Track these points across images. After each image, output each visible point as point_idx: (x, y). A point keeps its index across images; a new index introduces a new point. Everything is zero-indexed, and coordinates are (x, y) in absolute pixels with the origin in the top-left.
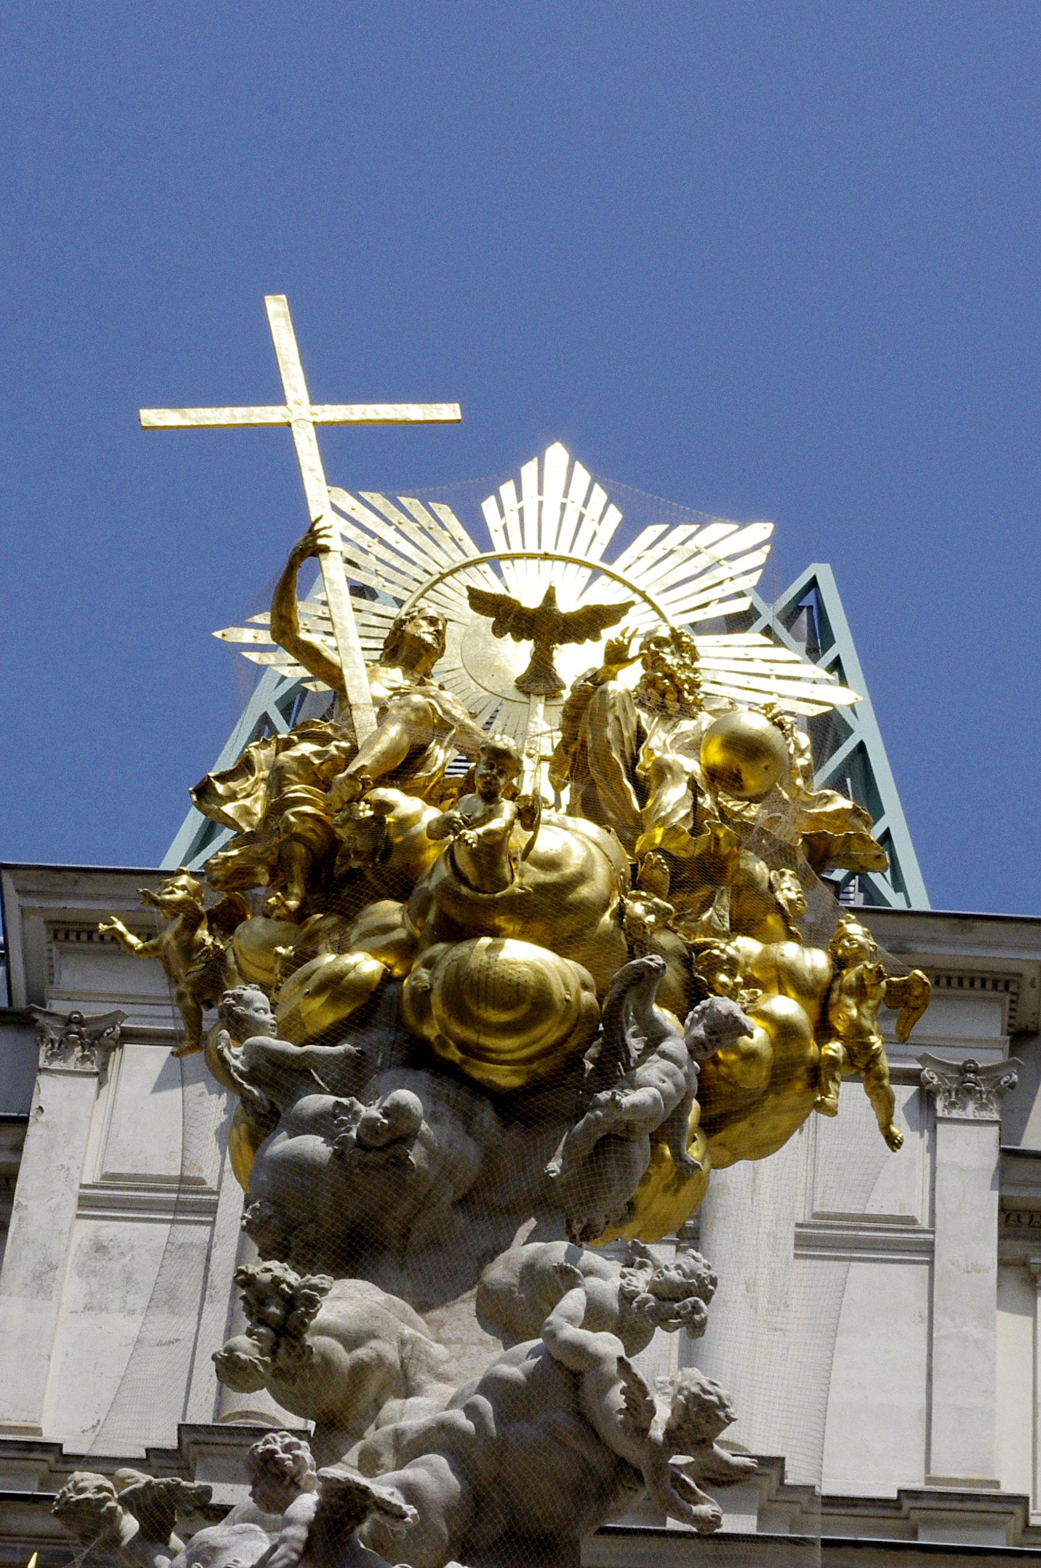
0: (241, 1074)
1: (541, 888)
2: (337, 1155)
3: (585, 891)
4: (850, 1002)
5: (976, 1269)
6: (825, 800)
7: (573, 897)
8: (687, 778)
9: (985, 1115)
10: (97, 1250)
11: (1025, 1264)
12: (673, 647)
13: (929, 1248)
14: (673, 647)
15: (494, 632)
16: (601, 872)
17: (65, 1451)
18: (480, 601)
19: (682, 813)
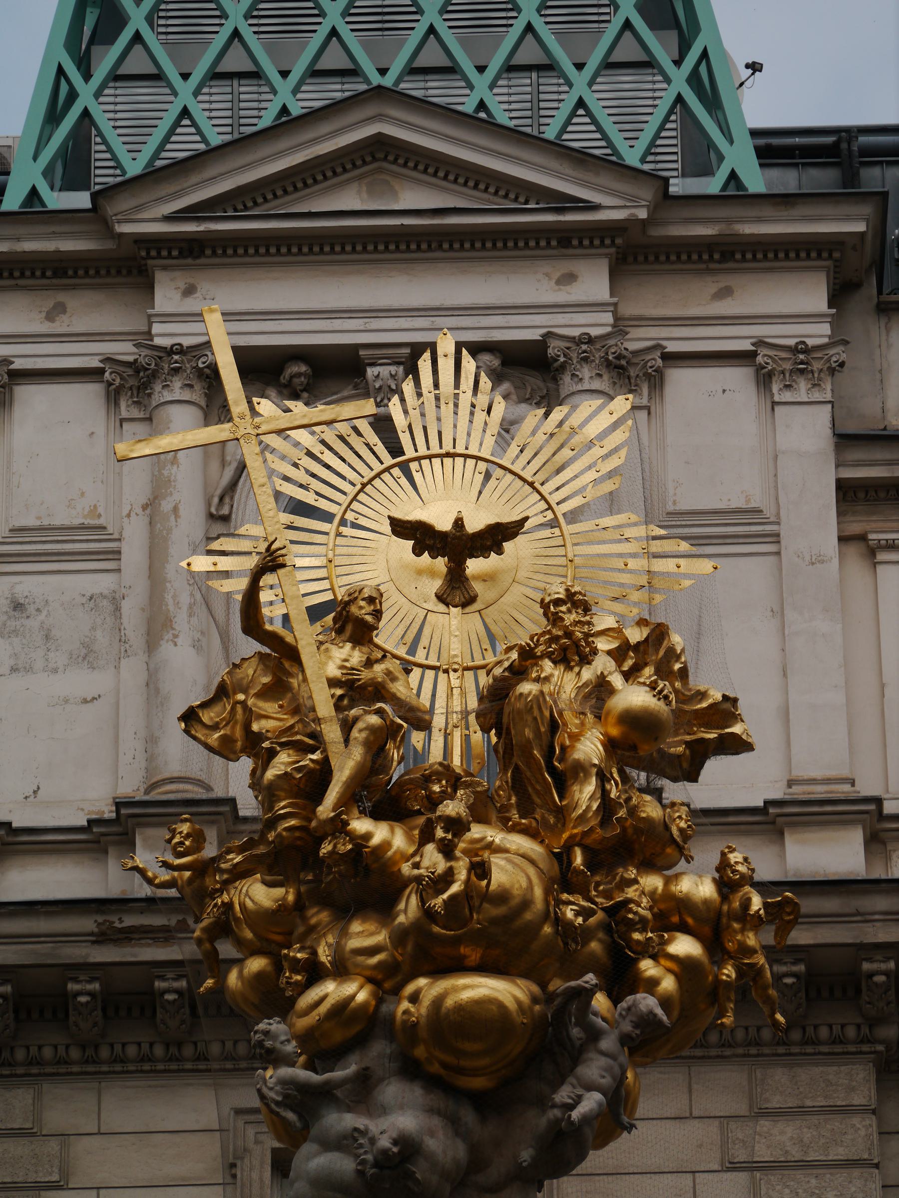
0: (277, 1103)
1: (495, 921)
2: (360, 1173)
3: (528, 916)
4: (736, 926)
5: (818, 560)
6: (699, 697)
7: (518, 923)
8: (595, 770)
9: (817, 396)
10: (15, 609)
11: (862, 538)
12: (569, 605)
13: (775, 538)
14: (569, 605)
15: (414, 552)
16: (538, 892)
17: (14, 825)
18: (401, 528)
19: (595, 806)
